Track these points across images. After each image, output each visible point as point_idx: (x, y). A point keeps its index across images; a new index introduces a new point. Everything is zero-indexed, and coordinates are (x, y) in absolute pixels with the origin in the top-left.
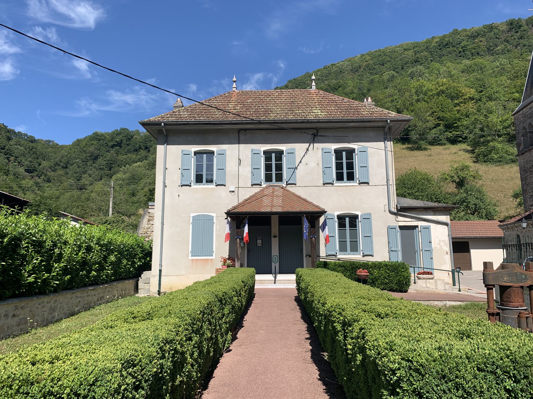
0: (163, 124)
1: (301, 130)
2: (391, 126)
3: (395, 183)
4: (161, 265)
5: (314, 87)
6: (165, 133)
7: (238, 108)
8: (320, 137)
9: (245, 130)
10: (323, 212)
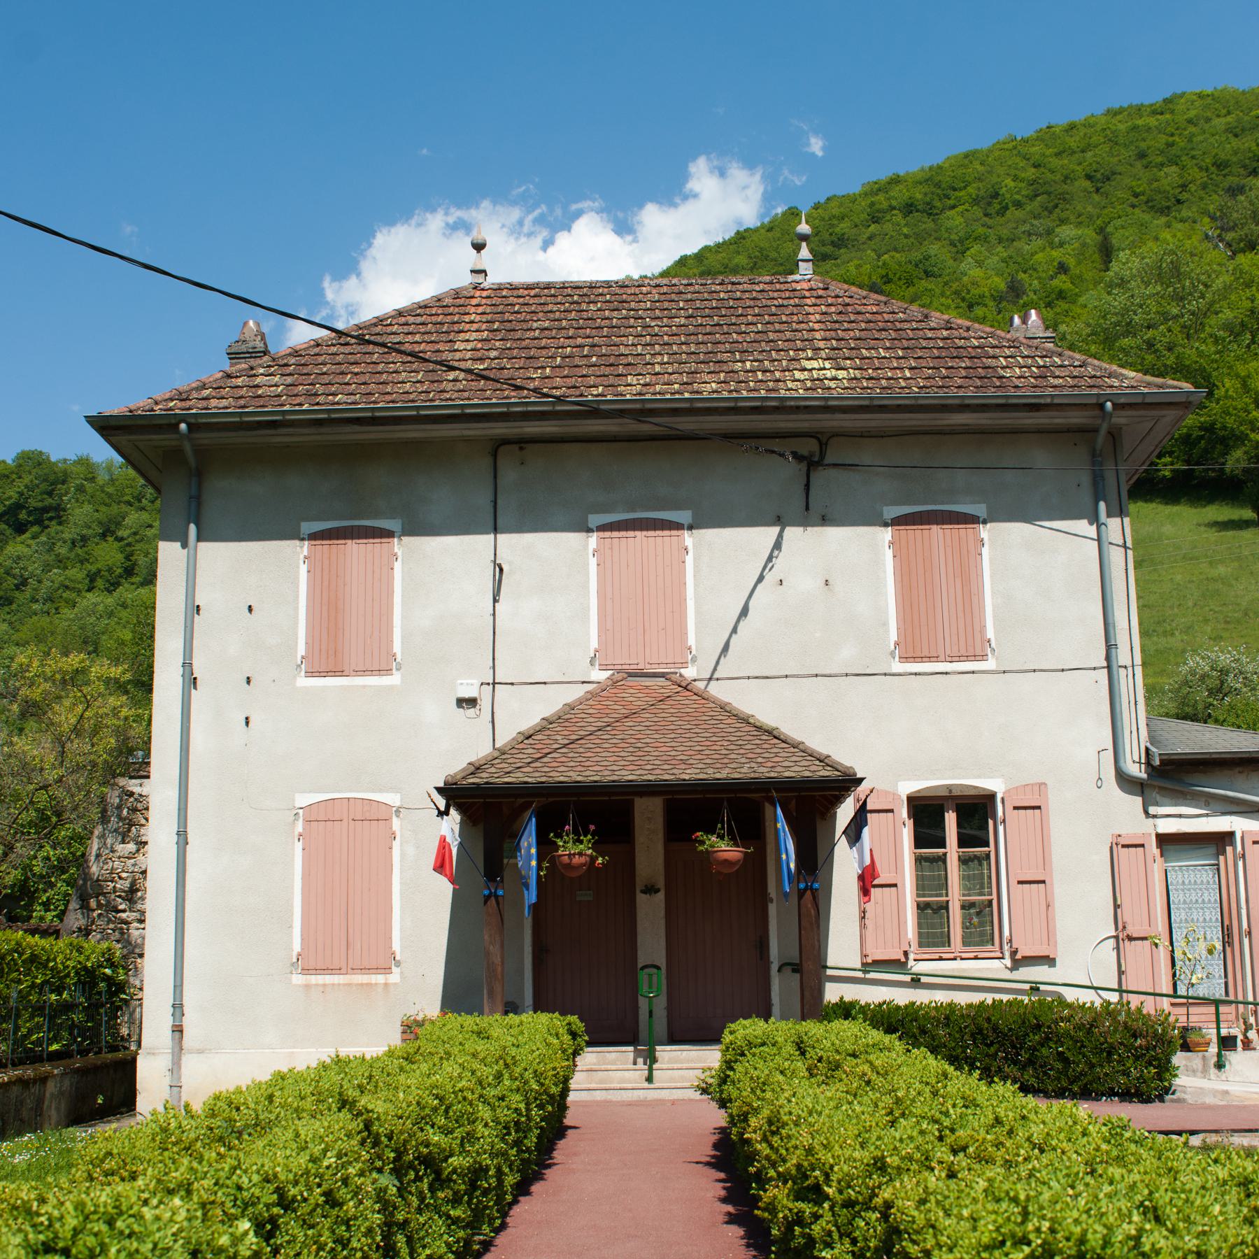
0: (183, 426)
1: (753, 443)
2: (1119, 428)
3: (1138, 660)
4: (178, 1008)
5: (806, 269)
6: (192, 460)
7: (493, 354)
8: (833, 472)
9: (522, 442)
10: (849, 782)
